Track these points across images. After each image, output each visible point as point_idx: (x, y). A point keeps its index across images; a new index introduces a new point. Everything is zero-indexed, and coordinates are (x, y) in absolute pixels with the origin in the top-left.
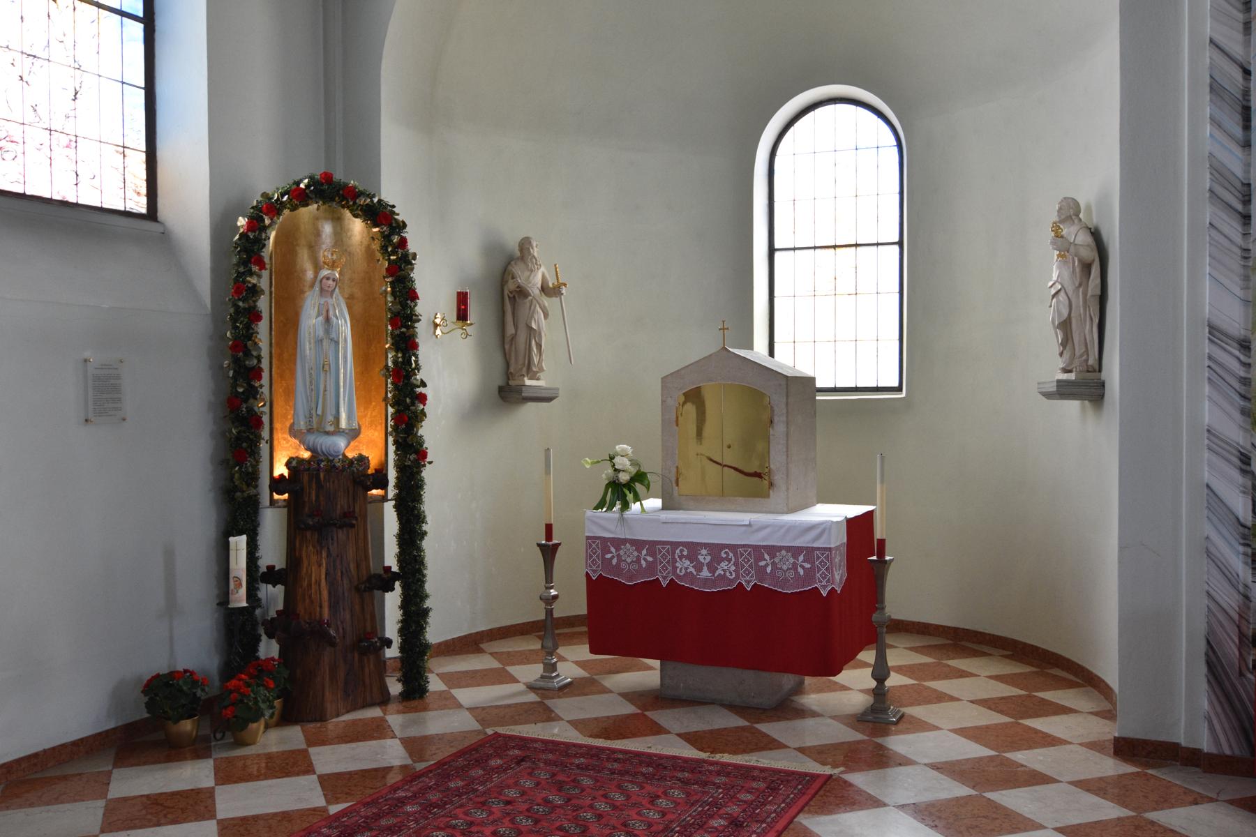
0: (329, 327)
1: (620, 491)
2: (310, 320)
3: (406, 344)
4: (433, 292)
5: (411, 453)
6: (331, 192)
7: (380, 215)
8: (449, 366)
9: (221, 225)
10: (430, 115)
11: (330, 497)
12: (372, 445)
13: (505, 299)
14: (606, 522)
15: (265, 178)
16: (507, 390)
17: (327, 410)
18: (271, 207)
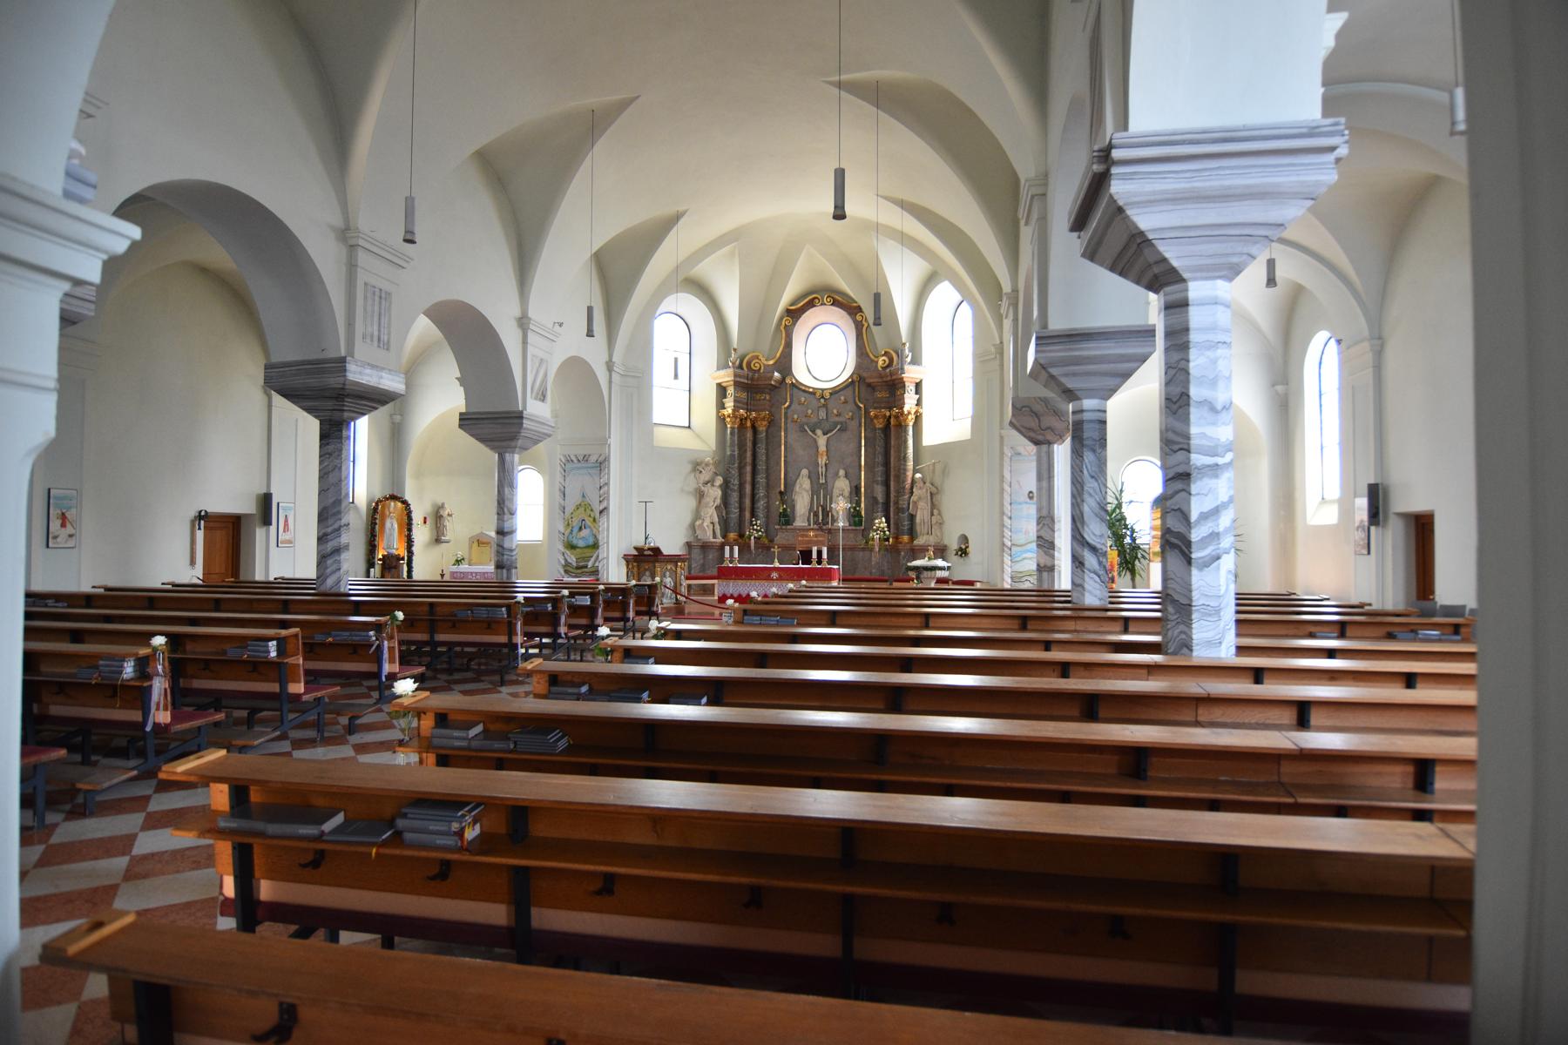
0: (392, 526)
1: (458, 562)
2: (388, 524)
3: (410, 530)
4: (417, 517)
5: (410, 553)
6: (393, 497)
7: (405, 502)
8: (421, 534)
9: (369, 505)
10: (419, 475)
11: (390, 564)
12: (403, 552)
13: (437, 518)
14: (455, 568)
15: (378, 495)
16: (438, 540)
17: (391, 543)
18: (379, 501)
